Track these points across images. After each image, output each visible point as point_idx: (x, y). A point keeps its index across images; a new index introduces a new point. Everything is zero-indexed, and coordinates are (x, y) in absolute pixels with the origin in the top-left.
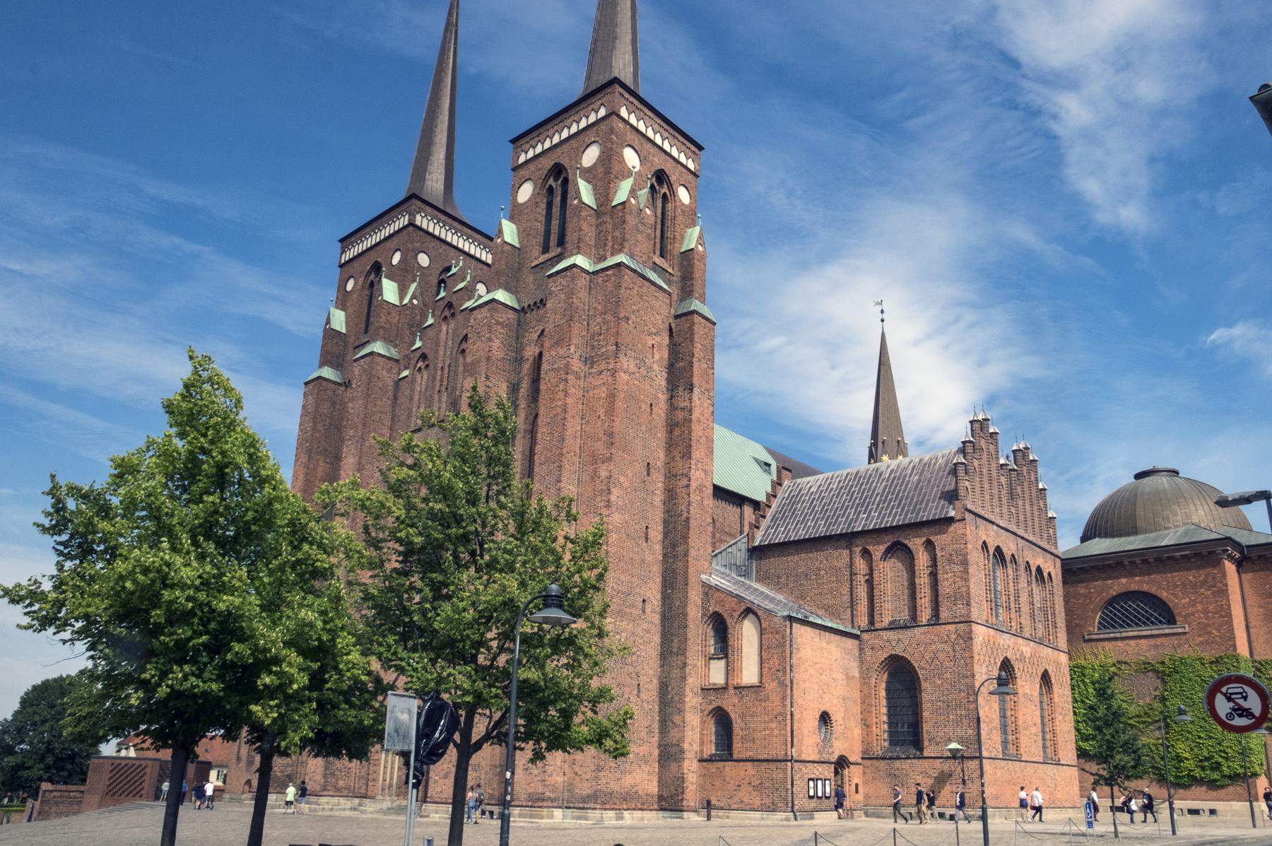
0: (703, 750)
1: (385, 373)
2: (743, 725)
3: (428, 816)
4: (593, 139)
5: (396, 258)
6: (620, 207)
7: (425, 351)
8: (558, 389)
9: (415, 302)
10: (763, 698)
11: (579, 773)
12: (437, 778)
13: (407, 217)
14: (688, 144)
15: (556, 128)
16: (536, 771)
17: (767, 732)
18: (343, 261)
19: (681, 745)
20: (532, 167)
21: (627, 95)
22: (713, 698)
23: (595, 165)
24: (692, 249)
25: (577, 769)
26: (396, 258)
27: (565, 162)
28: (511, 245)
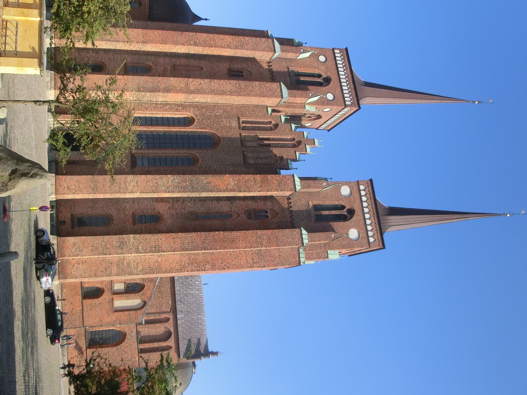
0: (86, 283)
2: (97, 304)
4: (360, 235)
5: (330, 96)
7: (279, 126)
8: (247, 242)
10: (108, 313)
11: (74, 267)
16: (74, 251)
17: (95, 316)
20: (357, 195)
22: (108, 287)
25: (75, 266)
27: (355, 218)
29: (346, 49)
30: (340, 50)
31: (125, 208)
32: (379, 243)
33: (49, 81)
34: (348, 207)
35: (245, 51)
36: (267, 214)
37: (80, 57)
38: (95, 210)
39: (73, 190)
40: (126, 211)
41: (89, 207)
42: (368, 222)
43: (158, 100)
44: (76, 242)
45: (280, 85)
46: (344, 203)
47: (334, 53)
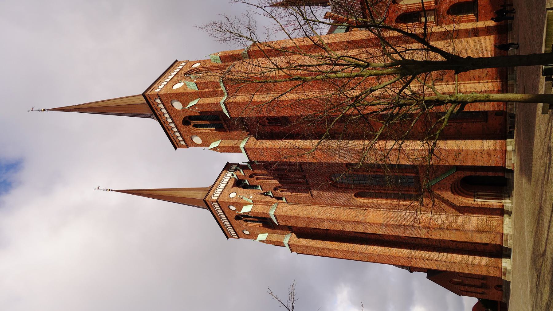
1: (284, 209)
3: (513, 164)
4: (170, 104)
5: (233, 208)
6: (198, 86)
7: (273, 189)
9: (251, 197)
11: (486, 73)
12: (491, 161)
13: (214, 204)
14: (174, 66)
15: (167, 125)
18: (237, 237)
19: (469, 30)
20: (186, 137)
21: (150, 90)
23: (181, 102)
24: (220, 57)
26: (233, 208)
27: (181, 118)
28: (220, 143)
29: (228, 238)
30: (233, 238)
31: (422, 128)
32: (150, 99)
33: (508, 241)
34: (191, 127)
35: (315, 245)
36: (268, 121)
37: (474, 246)
38: (458, 126)
39: (484, 153)
40: (421, 125)
41: (465, 128)
42: (167, 116)
43: (393, 212)
44: (482, 105)
45: (278, 224)
46: (195, 130)
47: (237, 235)
